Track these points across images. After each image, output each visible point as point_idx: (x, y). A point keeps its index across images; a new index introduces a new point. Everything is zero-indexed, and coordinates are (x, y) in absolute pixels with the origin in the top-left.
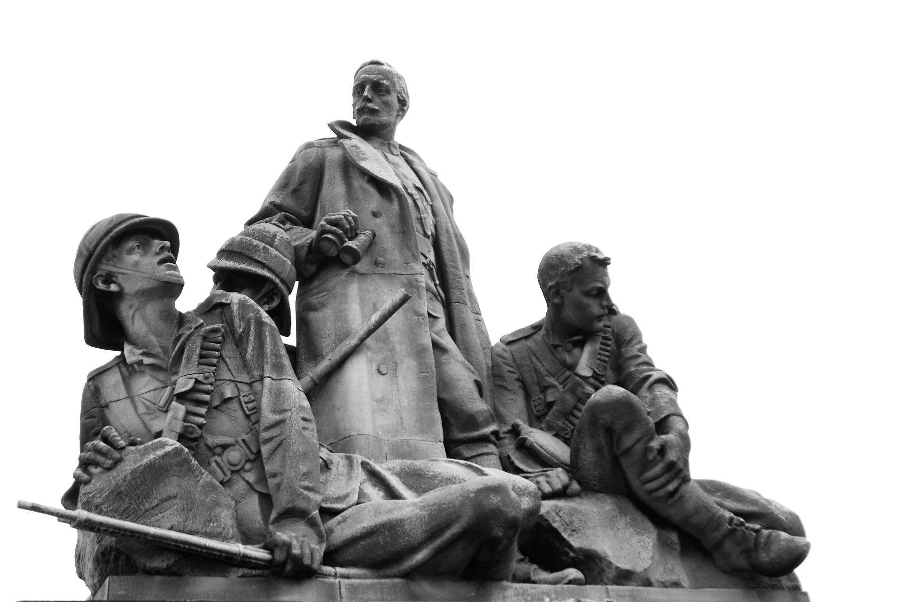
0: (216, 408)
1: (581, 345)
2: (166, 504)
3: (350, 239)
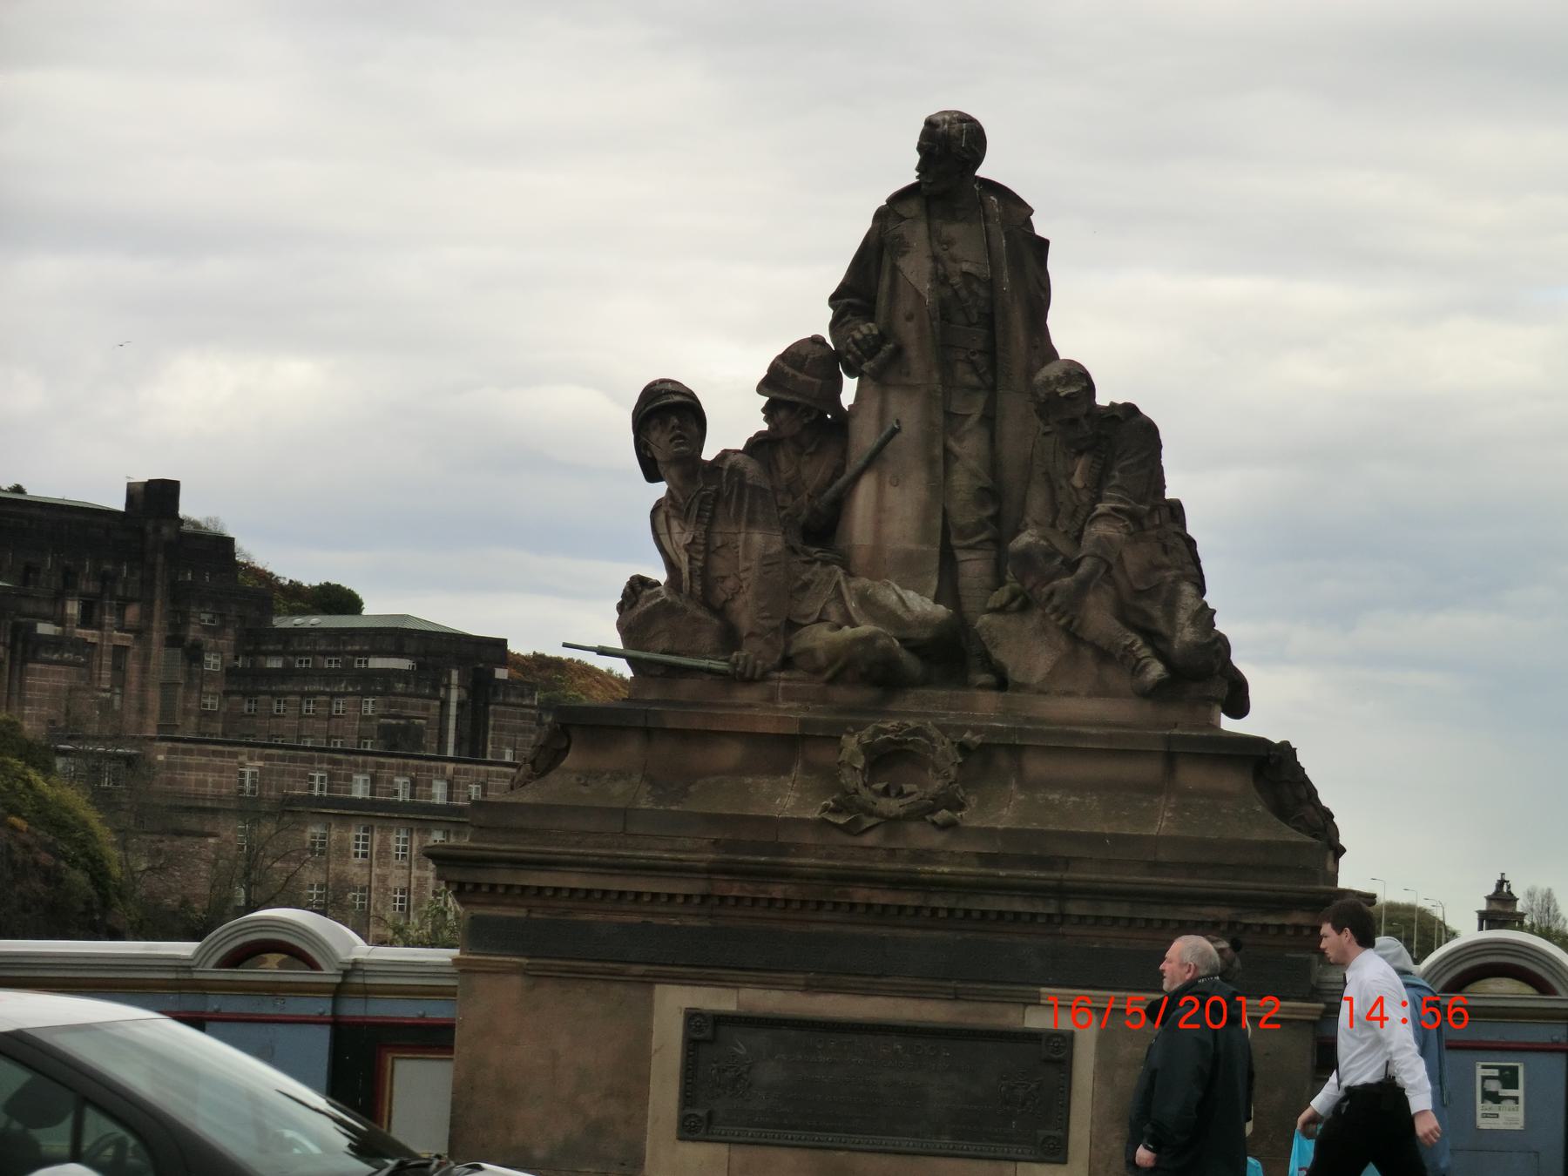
0: (713, 552)
3: (870, 359)
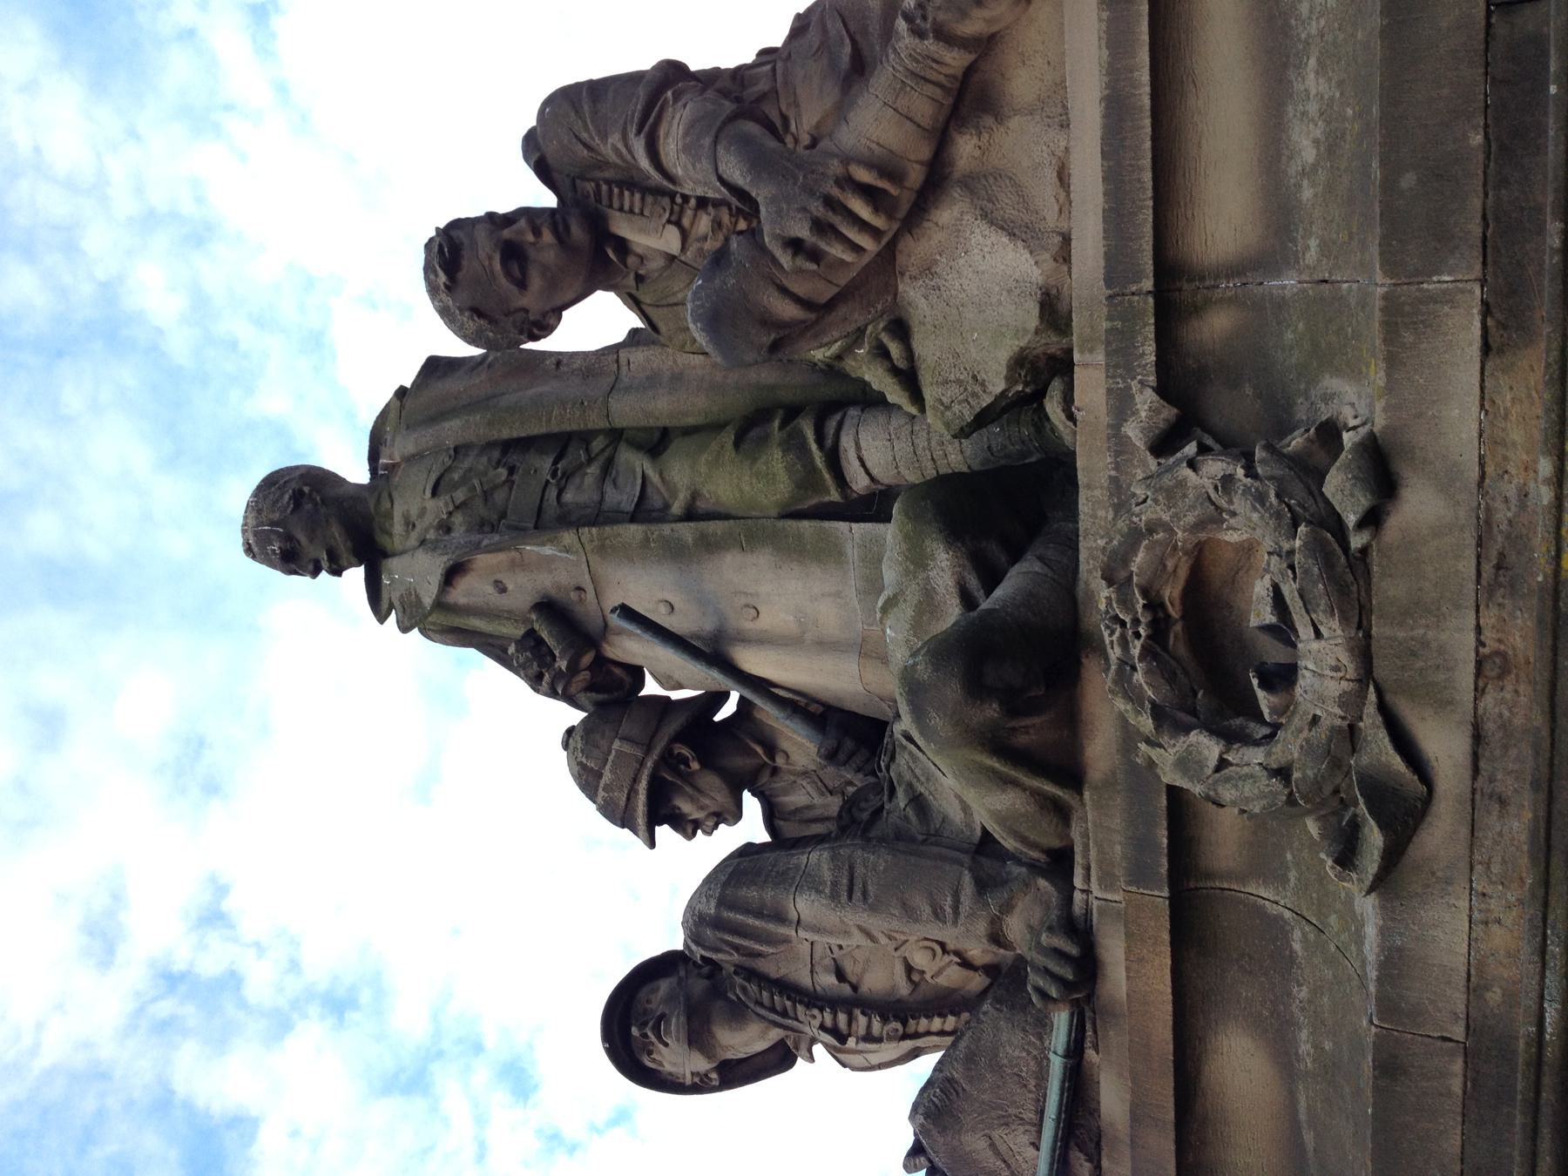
1: (622, 246)
2: (1002, 1148)
